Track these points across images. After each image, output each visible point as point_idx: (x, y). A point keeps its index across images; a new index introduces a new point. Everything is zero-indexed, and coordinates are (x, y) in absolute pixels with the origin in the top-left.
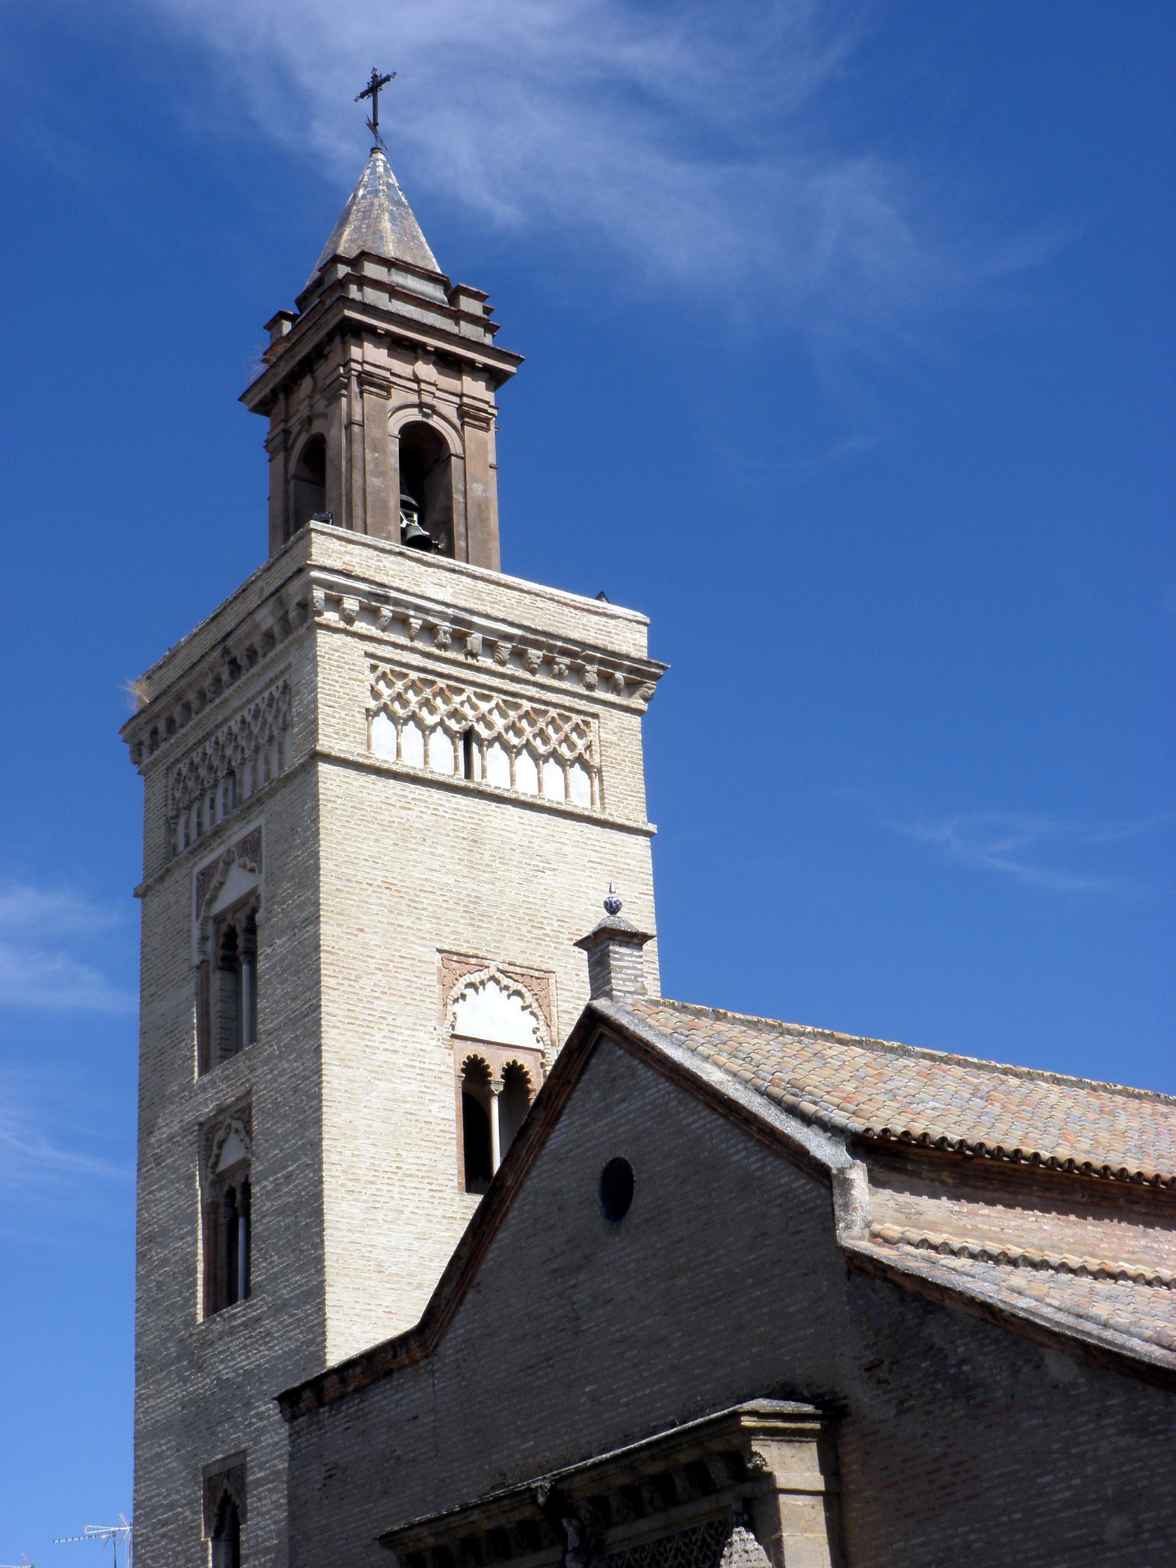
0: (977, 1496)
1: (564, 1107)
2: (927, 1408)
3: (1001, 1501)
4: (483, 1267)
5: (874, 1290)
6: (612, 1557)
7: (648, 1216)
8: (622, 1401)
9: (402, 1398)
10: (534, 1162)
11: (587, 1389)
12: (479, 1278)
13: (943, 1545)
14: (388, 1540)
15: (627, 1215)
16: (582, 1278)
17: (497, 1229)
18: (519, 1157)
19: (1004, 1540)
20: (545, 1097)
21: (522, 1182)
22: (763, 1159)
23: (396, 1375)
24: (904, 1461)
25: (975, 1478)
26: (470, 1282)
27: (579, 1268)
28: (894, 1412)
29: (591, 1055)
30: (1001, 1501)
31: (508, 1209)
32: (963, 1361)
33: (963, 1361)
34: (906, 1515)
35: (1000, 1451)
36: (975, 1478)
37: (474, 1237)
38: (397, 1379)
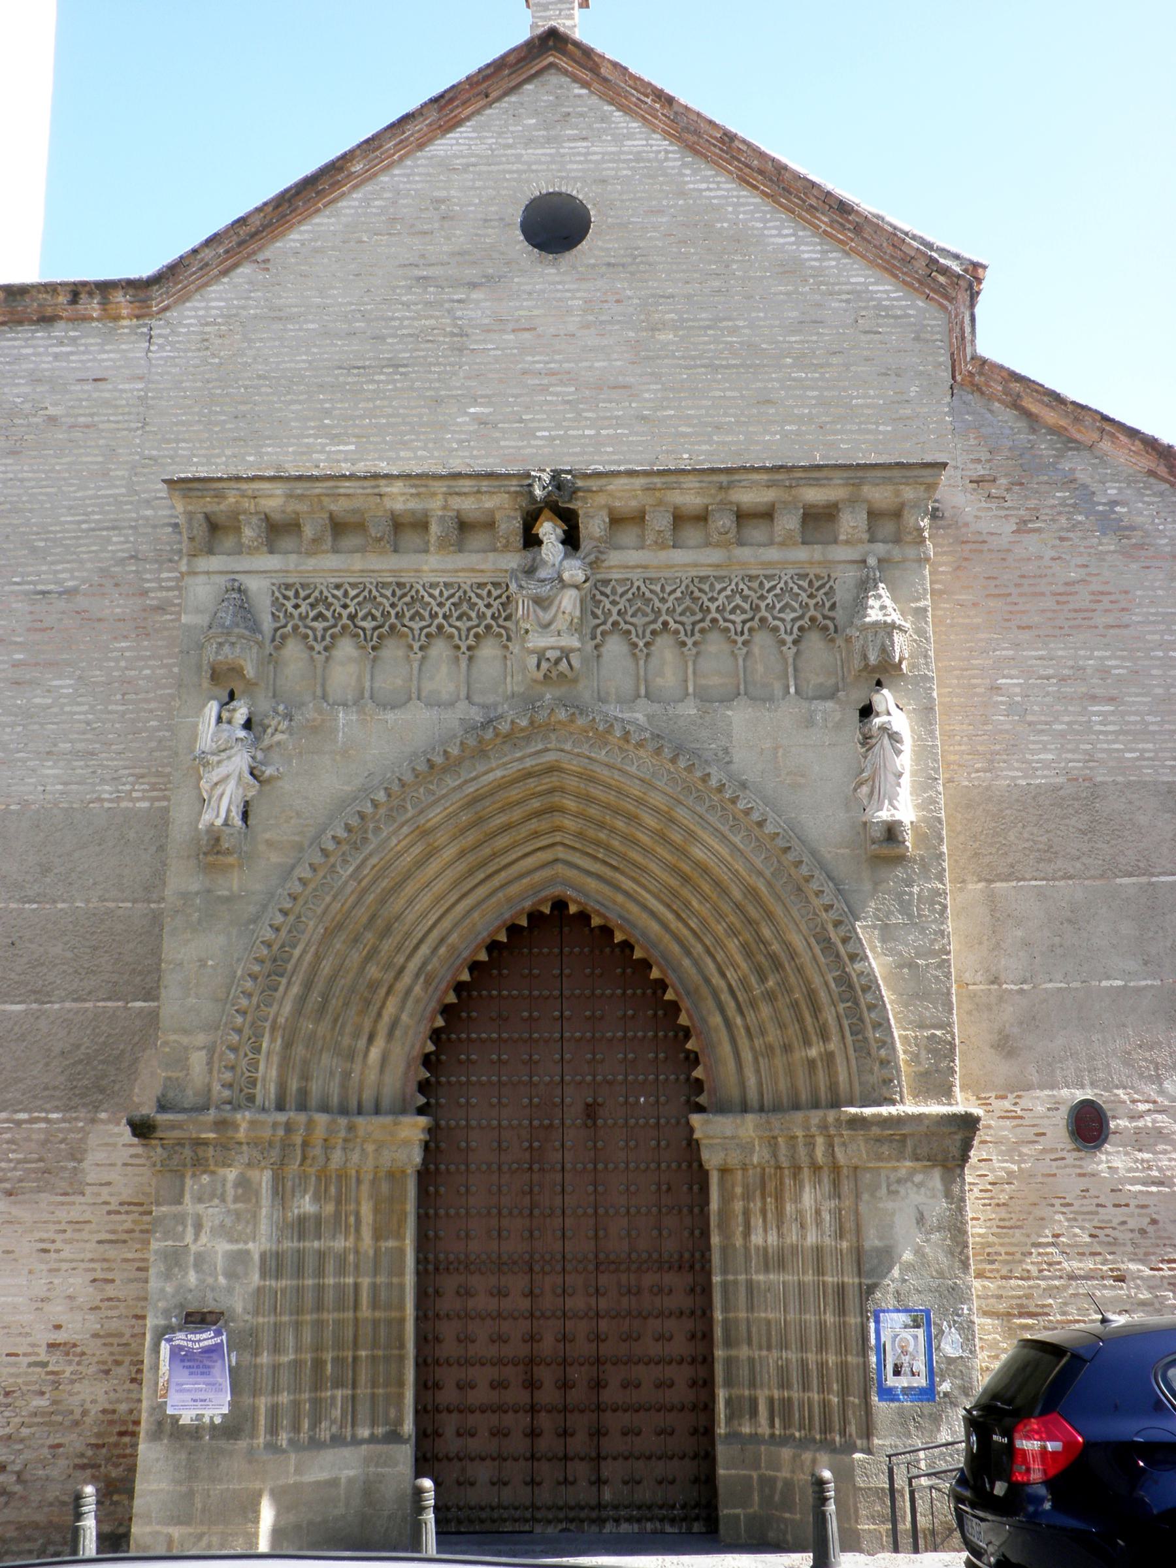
0: (1127, 626)
1: (468, 118)
2: (1063, 534)
3: (1157, 637)
4: (278, 244)
5: (991, 411)
6: (606, 582)
7: (613, 260)
8: (539, 434)
9: (72, 353)
10: (401, 159)
11: (472, 410)
12: (267, 254)
13: (1071, 663)
14: (182, 486)
15: (575, 251)
16: (475, 295)
17: (318, 210)
18: (381, 146)
19: (1155, 672)
20: (447, 97)
21: (375, 175)
22: (823, 252)
23: (61, 325)
24: (1023, 576)
25: (1123, 610)
26: (254, 253)
27: (474, 286)
28: (1014, 527)
29: (528, 80)
30: (1157, 637)
31: (343, 194)
32: (1115, 503)
33: (1115, 503)
34: (1019, 627)
35: (1160, 592)
36: (1123, 610)
37: (277, 207)
38: (59, 330)
